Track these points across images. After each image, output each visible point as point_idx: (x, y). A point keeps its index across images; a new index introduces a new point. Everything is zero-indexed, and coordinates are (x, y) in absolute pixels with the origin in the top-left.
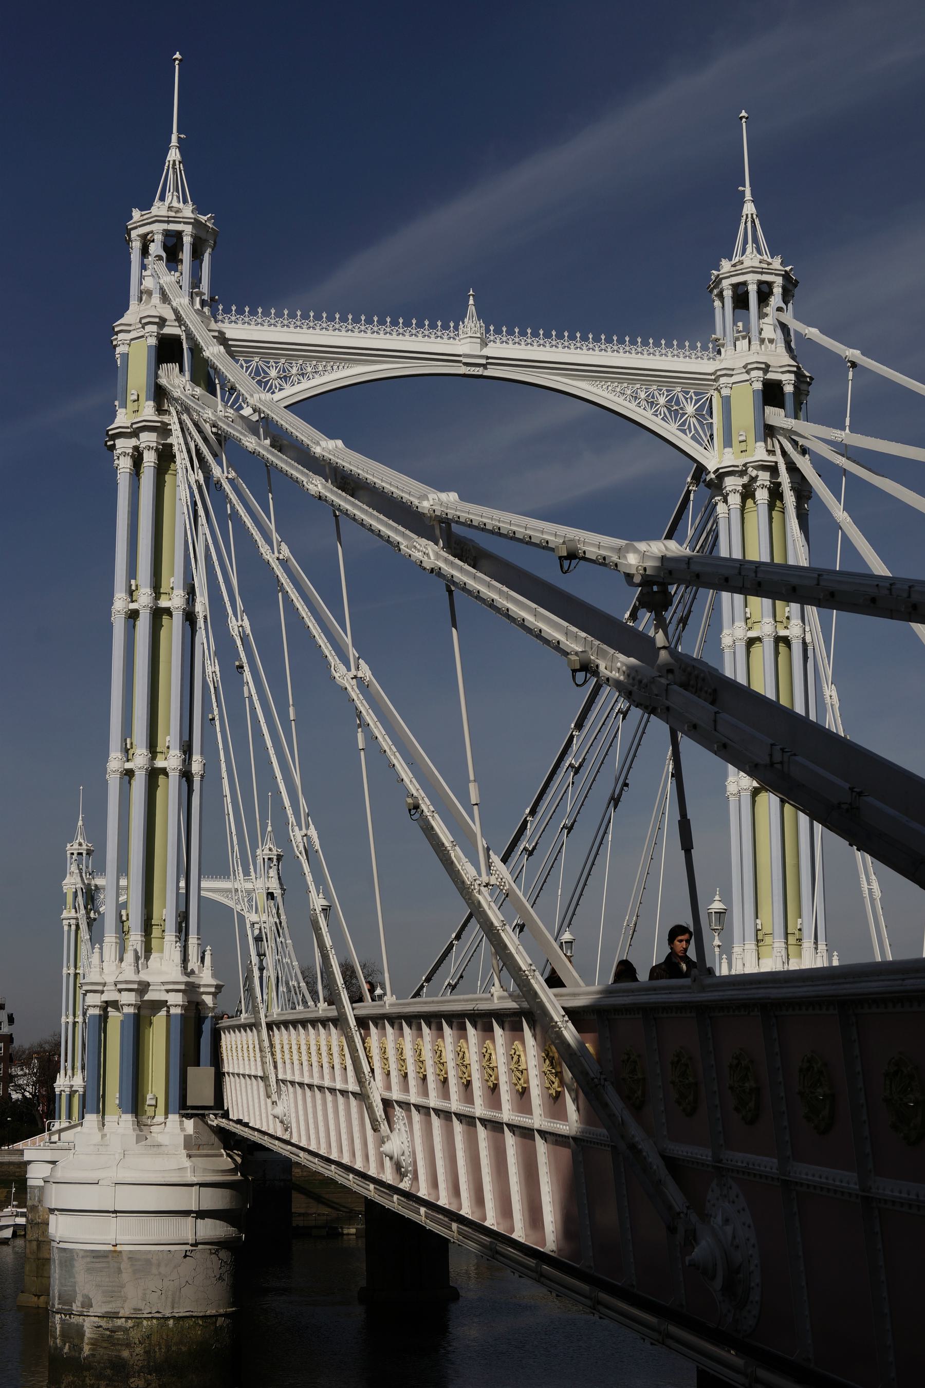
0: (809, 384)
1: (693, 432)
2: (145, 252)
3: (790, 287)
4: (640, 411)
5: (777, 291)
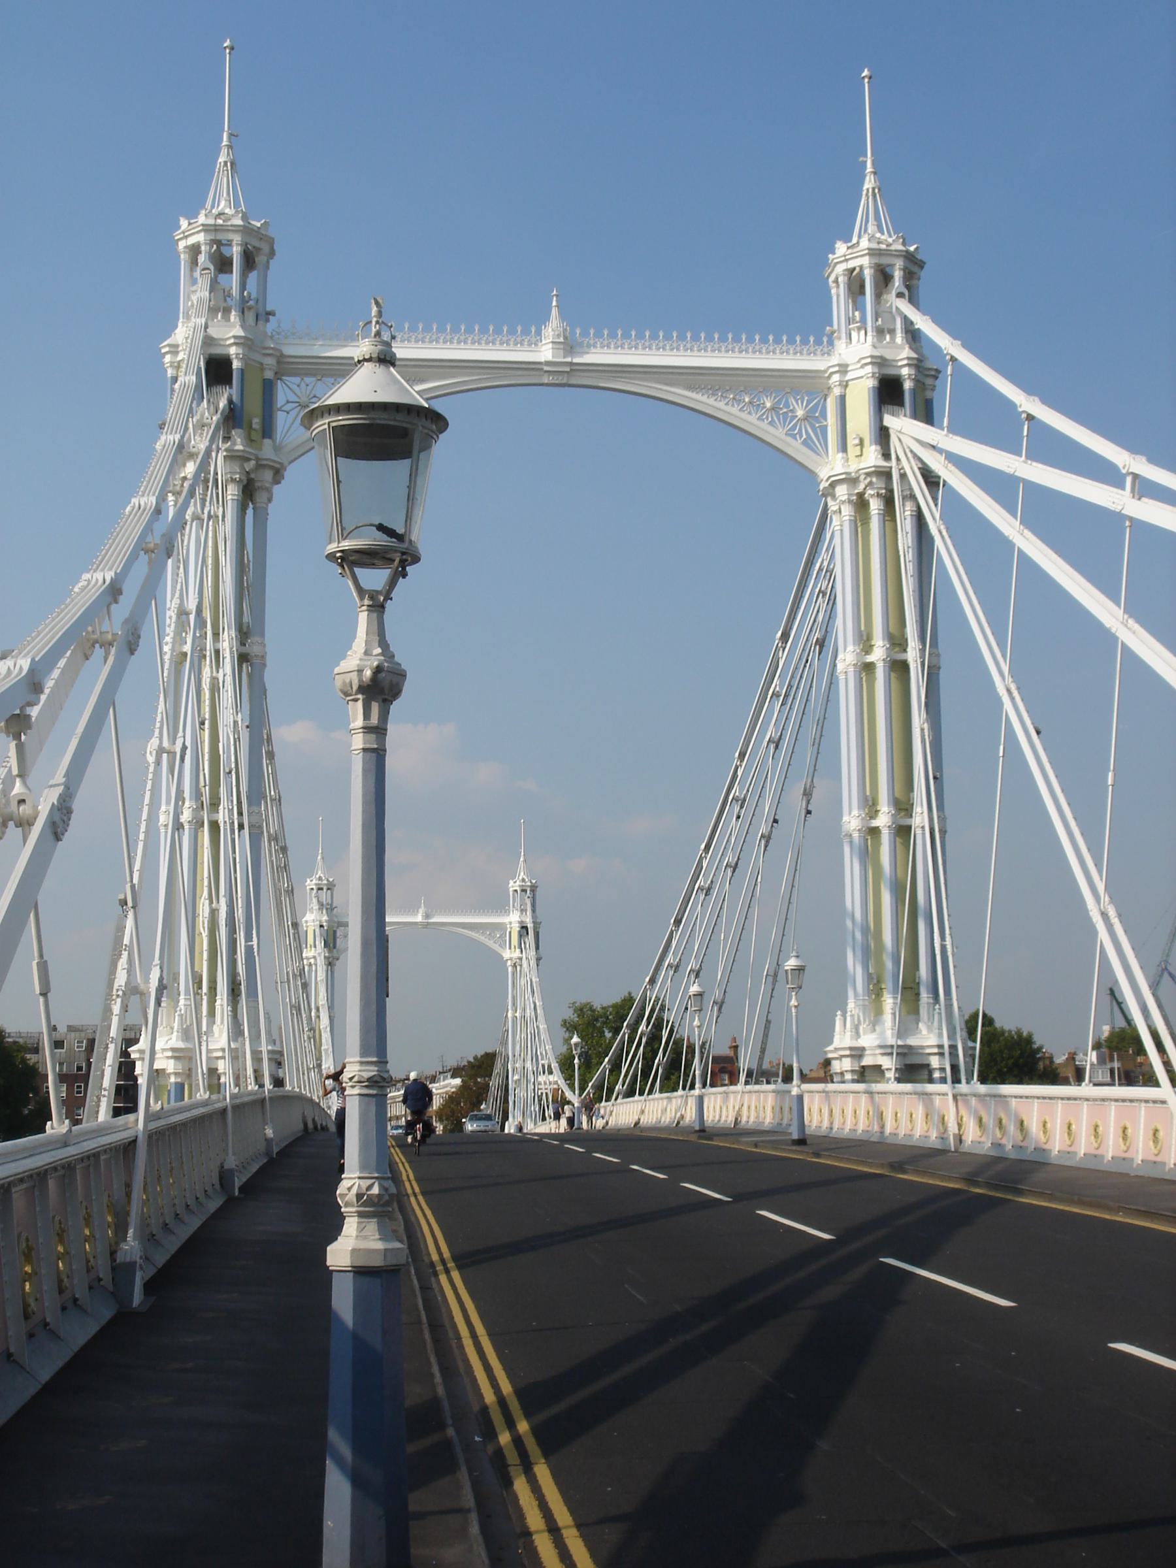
0: (936, 378)
1: (804, 436)
2: (194, 262)
3: (915, 269)
4: (744, 415)
5: (898, 275)
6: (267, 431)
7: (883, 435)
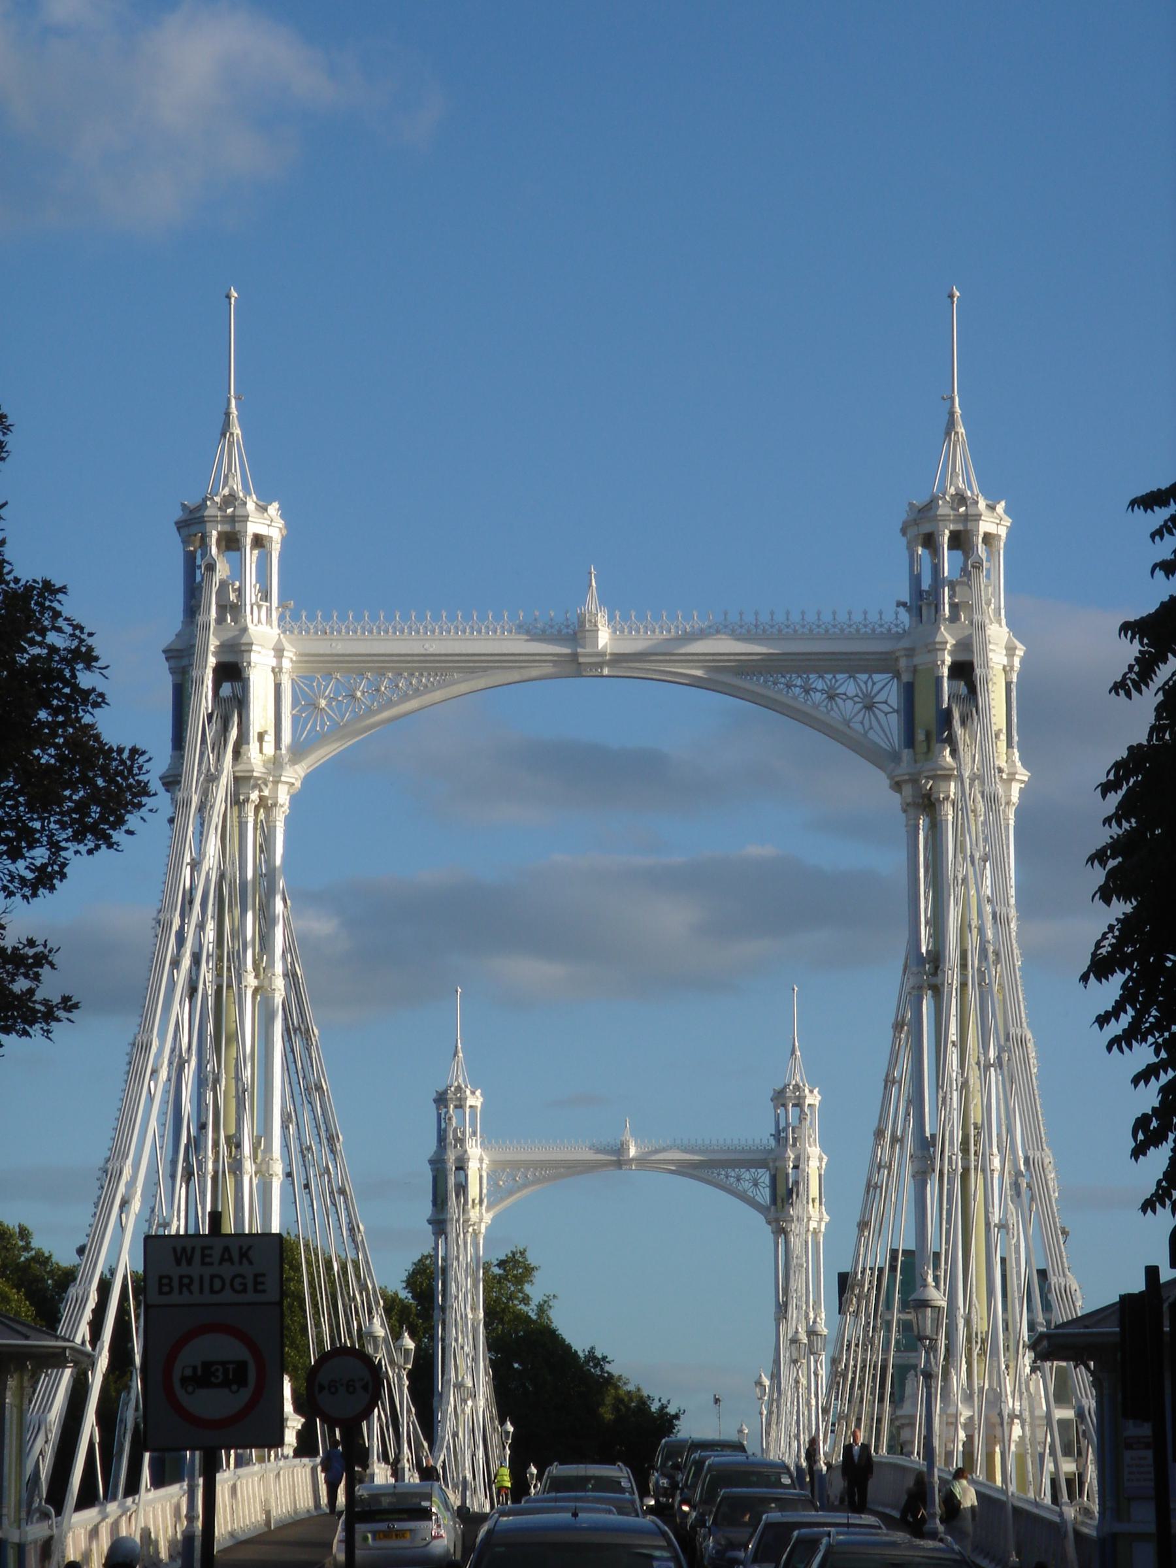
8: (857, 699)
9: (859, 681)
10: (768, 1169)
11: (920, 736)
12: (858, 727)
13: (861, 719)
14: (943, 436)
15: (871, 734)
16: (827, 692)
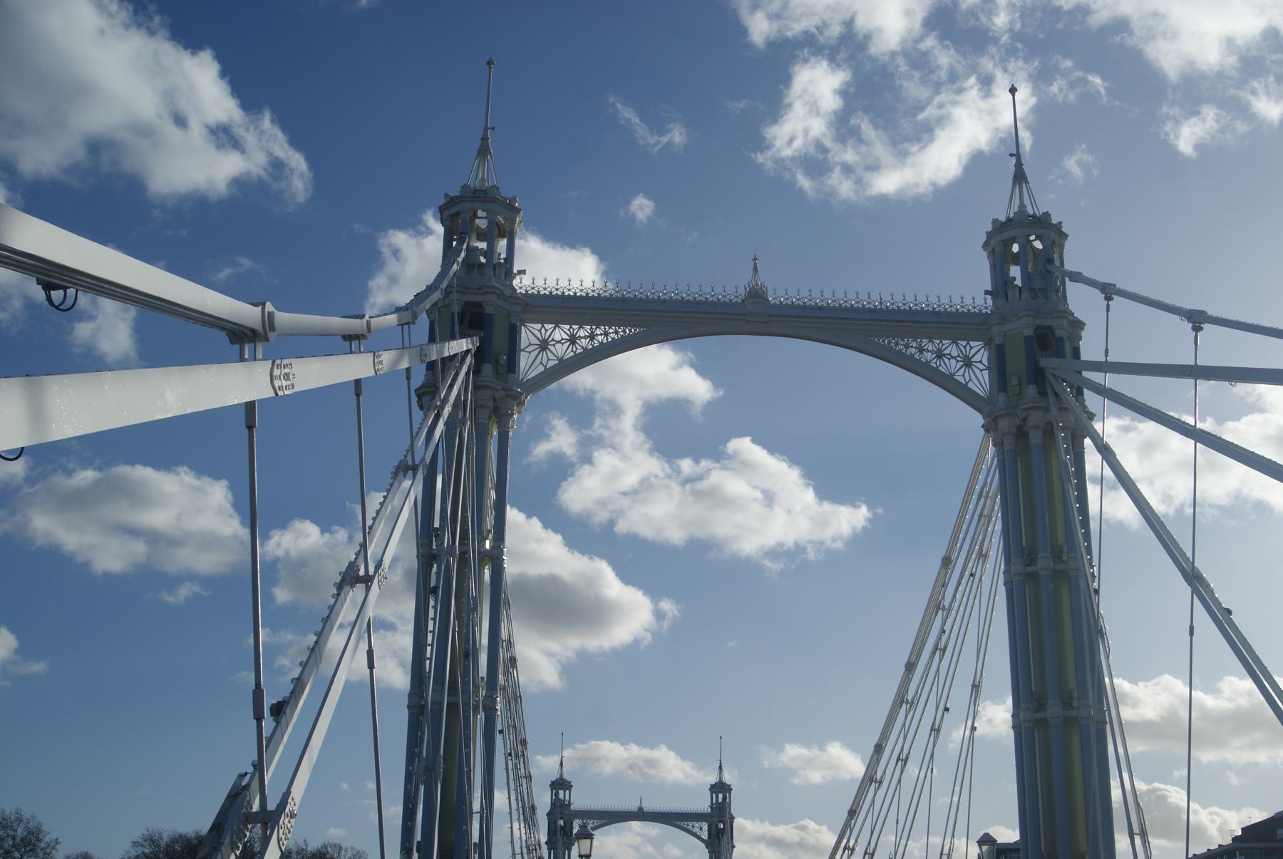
6: (512, 365)
7: (1038, 376)
8: (958, 359)
9: (961, 347)
10: (708, 822)
11: (1014, 381)
12: (961, 380)
13: (962, 373)
14: (1011, 182)
15: (971, 385)
16: (936, 353)
